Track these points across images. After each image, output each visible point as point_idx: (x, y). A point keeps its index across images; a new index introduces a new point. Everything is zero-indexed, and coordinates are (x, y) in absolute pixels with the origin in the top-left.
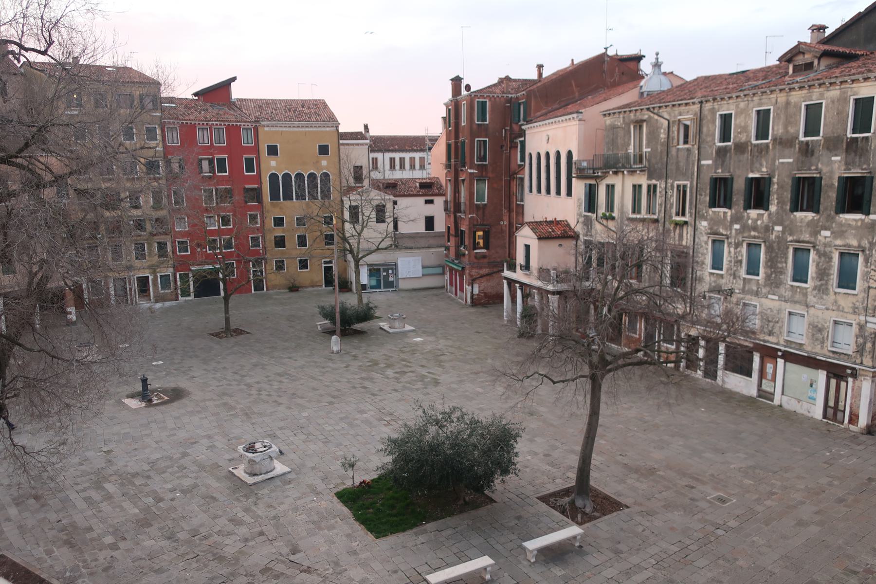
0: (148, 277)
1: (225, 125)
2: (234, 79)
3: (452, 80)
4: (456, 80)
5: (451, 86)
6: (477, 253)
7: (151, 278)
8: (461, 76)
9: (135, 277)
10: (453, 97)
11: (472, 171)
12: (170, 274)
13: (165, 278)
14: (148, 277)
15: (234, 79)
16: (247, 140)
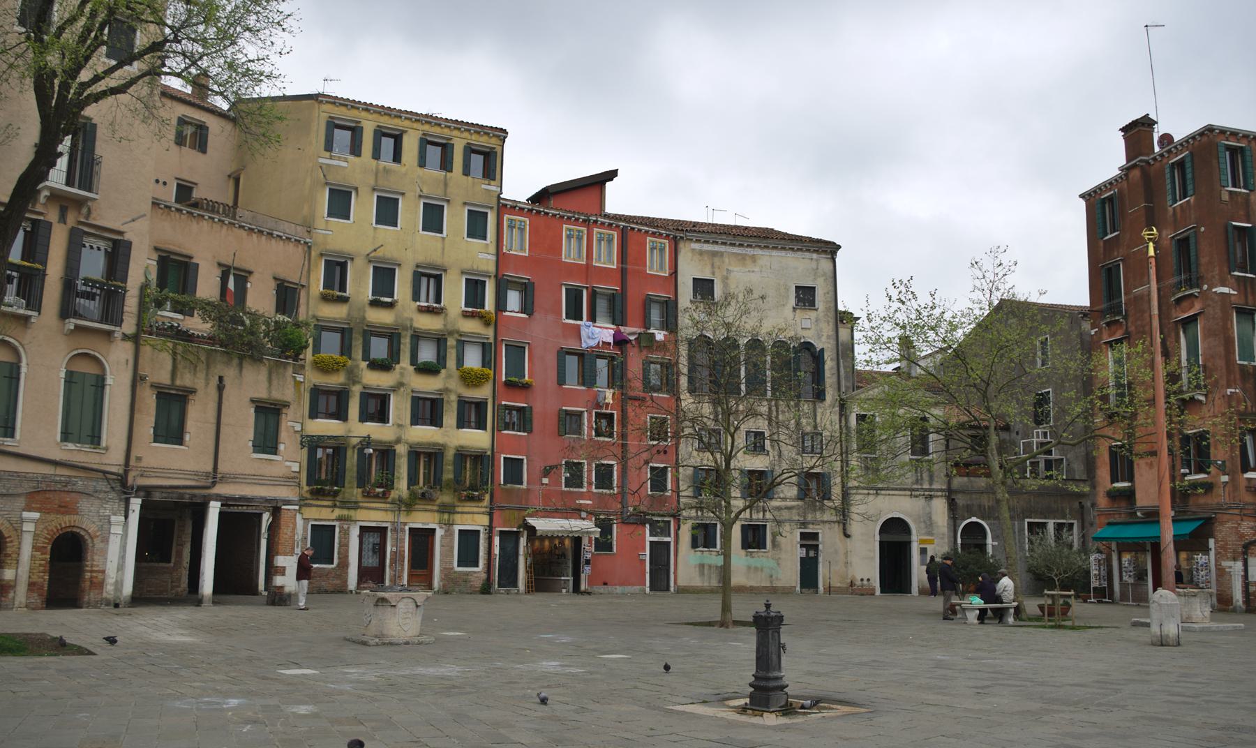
0: (433, 530)
1: (618, 226)
2: (612, 175)
3: (1122, 130)
4: (1143, 124)
5: (1122, 142)
6: (1249, 480)
7: (439, 533)
8: (1153, 116)
9: (407, 528)
10: (1128, 160)
11: (1225, 290)
12: (481, 529)
13: (468, 538)
14: (433, 530)
15: (612, 175)
16: (655, 265)
